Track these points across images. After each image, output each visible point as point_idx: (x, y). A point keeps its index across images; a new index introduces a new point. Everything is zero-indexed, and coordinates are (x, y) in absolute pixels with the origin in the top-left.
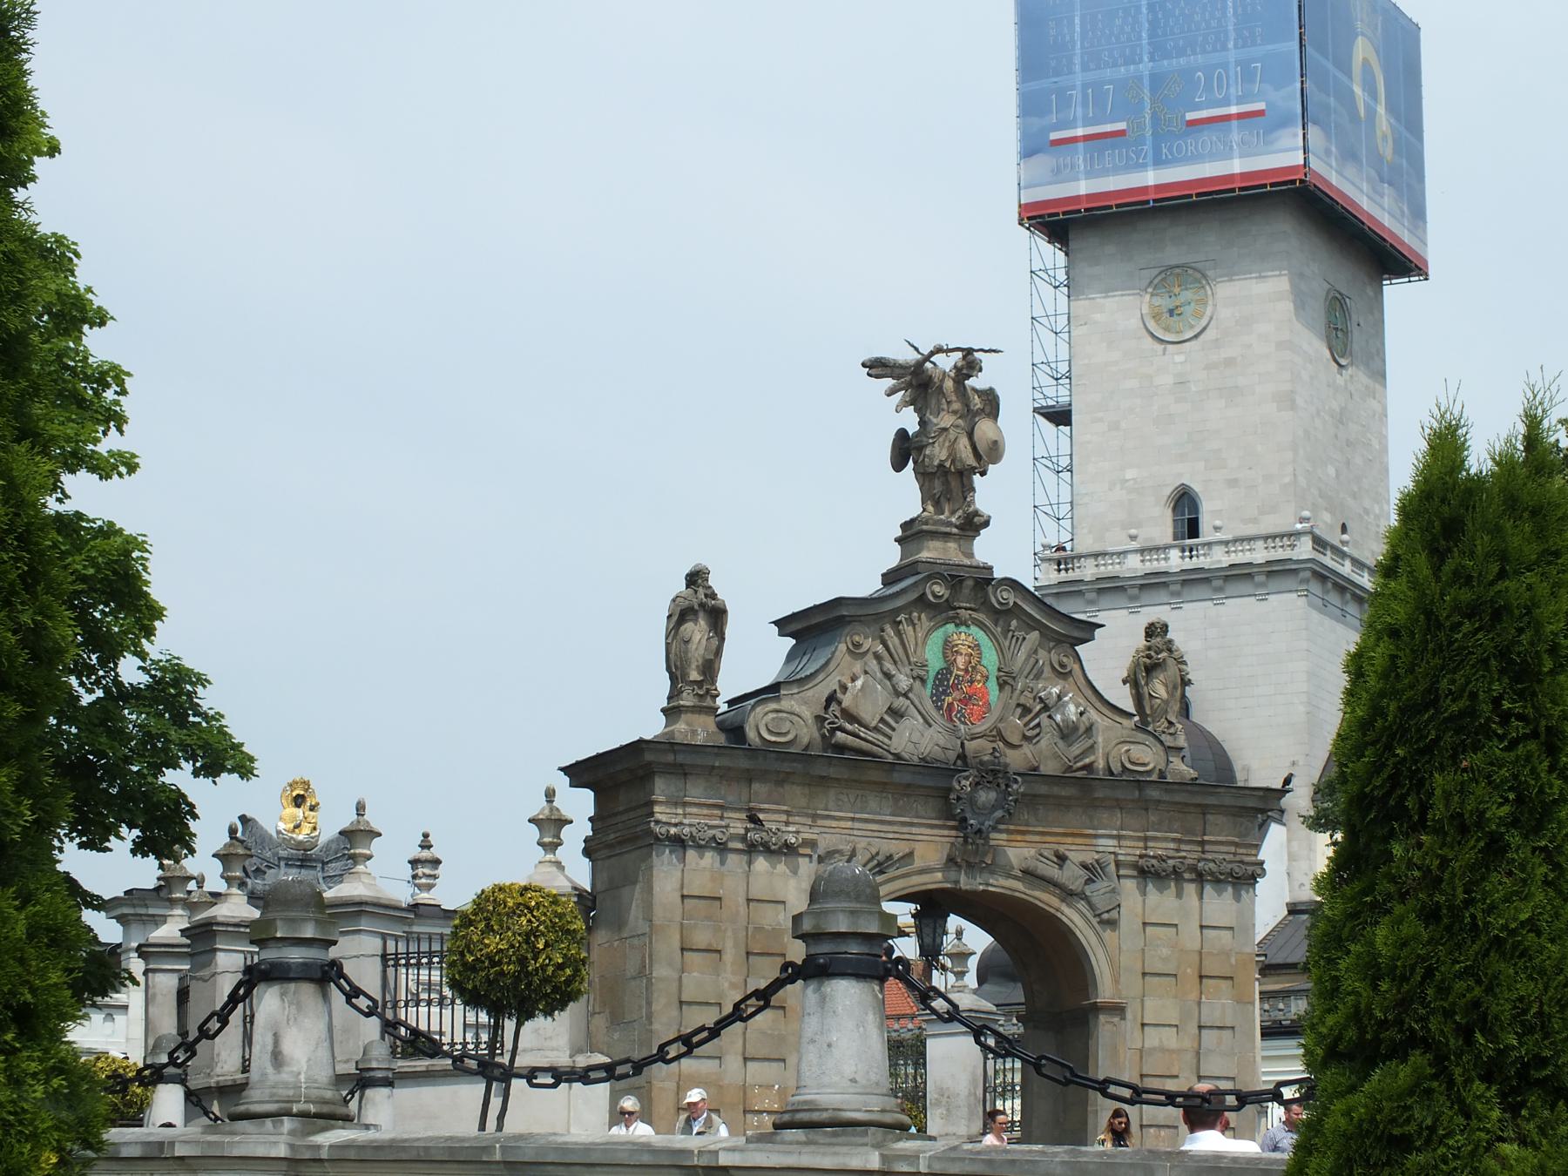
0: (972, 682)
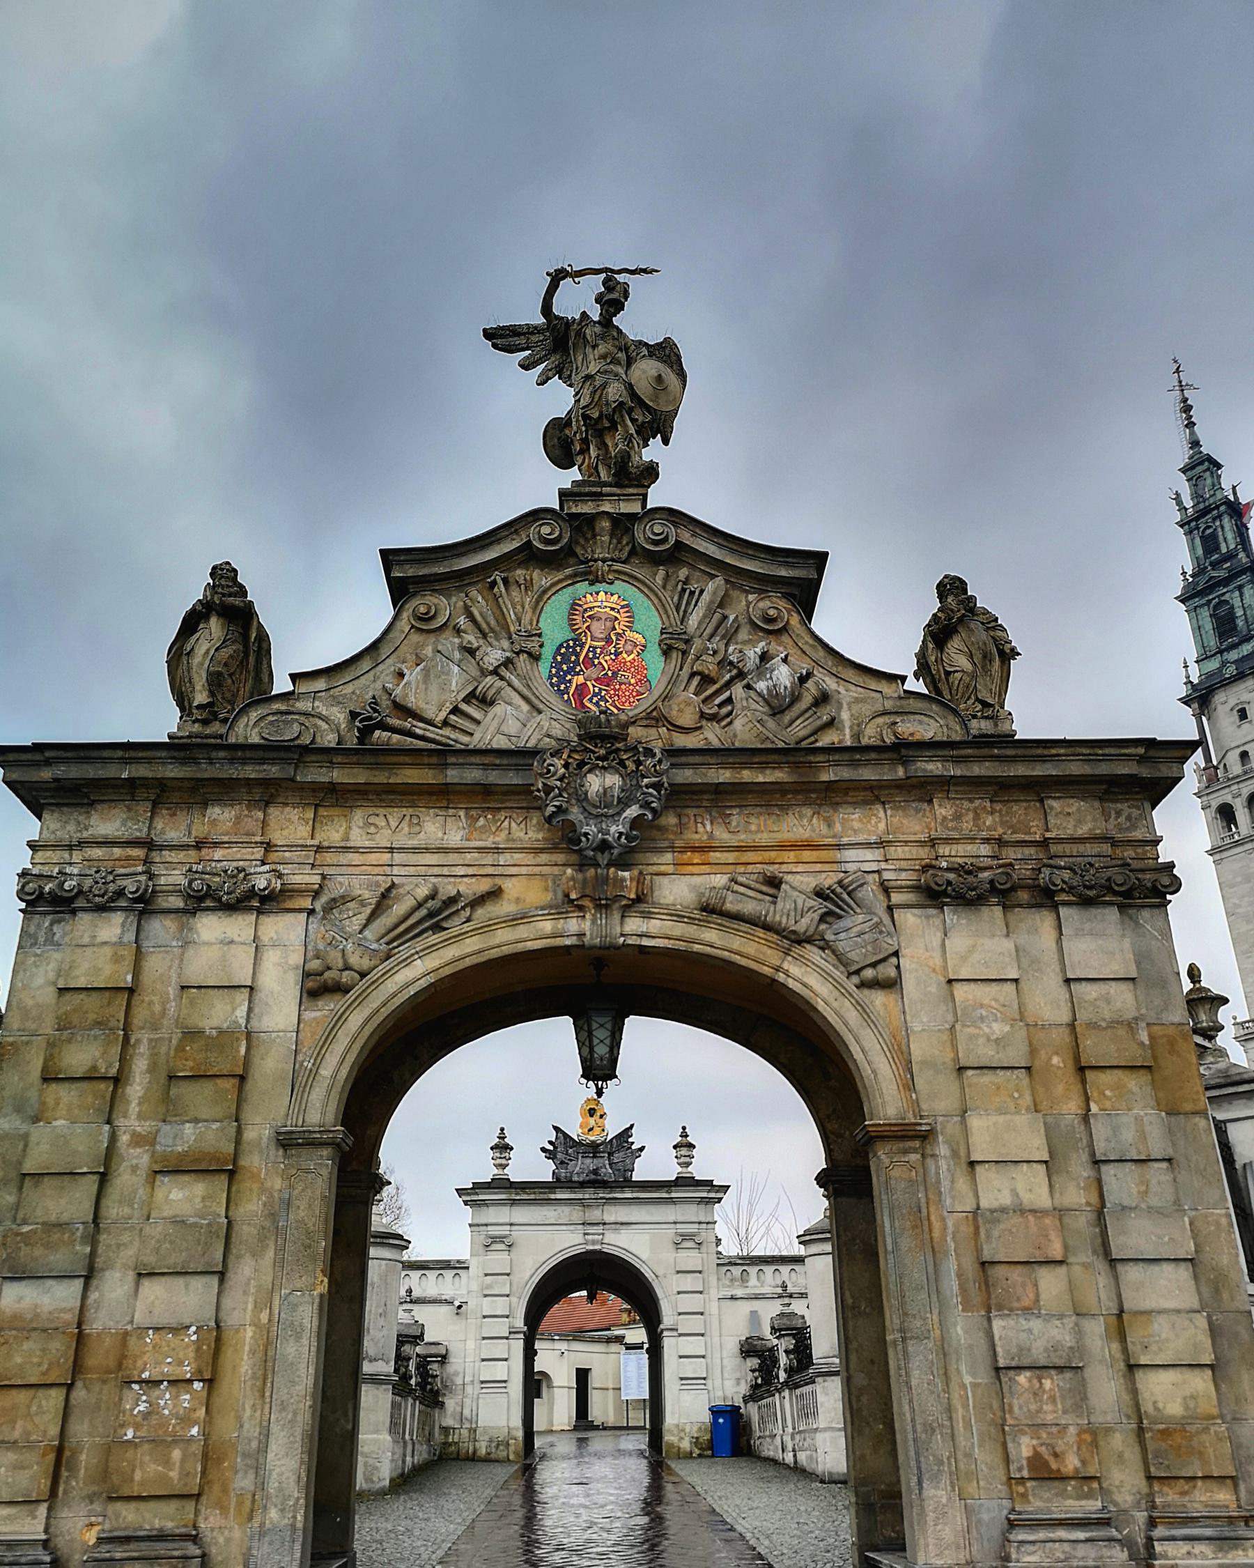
0: (617, 654)
